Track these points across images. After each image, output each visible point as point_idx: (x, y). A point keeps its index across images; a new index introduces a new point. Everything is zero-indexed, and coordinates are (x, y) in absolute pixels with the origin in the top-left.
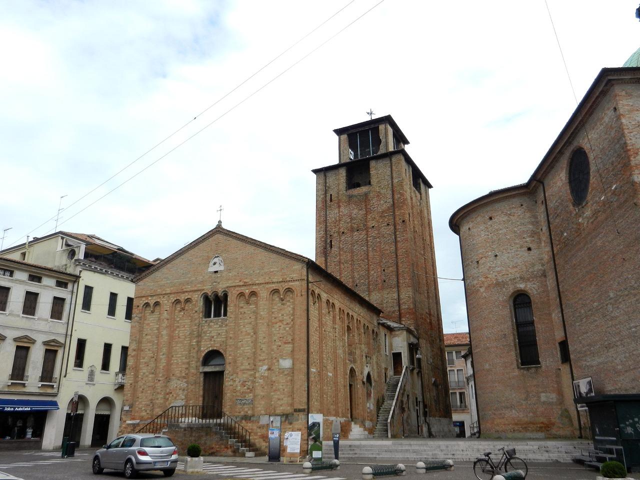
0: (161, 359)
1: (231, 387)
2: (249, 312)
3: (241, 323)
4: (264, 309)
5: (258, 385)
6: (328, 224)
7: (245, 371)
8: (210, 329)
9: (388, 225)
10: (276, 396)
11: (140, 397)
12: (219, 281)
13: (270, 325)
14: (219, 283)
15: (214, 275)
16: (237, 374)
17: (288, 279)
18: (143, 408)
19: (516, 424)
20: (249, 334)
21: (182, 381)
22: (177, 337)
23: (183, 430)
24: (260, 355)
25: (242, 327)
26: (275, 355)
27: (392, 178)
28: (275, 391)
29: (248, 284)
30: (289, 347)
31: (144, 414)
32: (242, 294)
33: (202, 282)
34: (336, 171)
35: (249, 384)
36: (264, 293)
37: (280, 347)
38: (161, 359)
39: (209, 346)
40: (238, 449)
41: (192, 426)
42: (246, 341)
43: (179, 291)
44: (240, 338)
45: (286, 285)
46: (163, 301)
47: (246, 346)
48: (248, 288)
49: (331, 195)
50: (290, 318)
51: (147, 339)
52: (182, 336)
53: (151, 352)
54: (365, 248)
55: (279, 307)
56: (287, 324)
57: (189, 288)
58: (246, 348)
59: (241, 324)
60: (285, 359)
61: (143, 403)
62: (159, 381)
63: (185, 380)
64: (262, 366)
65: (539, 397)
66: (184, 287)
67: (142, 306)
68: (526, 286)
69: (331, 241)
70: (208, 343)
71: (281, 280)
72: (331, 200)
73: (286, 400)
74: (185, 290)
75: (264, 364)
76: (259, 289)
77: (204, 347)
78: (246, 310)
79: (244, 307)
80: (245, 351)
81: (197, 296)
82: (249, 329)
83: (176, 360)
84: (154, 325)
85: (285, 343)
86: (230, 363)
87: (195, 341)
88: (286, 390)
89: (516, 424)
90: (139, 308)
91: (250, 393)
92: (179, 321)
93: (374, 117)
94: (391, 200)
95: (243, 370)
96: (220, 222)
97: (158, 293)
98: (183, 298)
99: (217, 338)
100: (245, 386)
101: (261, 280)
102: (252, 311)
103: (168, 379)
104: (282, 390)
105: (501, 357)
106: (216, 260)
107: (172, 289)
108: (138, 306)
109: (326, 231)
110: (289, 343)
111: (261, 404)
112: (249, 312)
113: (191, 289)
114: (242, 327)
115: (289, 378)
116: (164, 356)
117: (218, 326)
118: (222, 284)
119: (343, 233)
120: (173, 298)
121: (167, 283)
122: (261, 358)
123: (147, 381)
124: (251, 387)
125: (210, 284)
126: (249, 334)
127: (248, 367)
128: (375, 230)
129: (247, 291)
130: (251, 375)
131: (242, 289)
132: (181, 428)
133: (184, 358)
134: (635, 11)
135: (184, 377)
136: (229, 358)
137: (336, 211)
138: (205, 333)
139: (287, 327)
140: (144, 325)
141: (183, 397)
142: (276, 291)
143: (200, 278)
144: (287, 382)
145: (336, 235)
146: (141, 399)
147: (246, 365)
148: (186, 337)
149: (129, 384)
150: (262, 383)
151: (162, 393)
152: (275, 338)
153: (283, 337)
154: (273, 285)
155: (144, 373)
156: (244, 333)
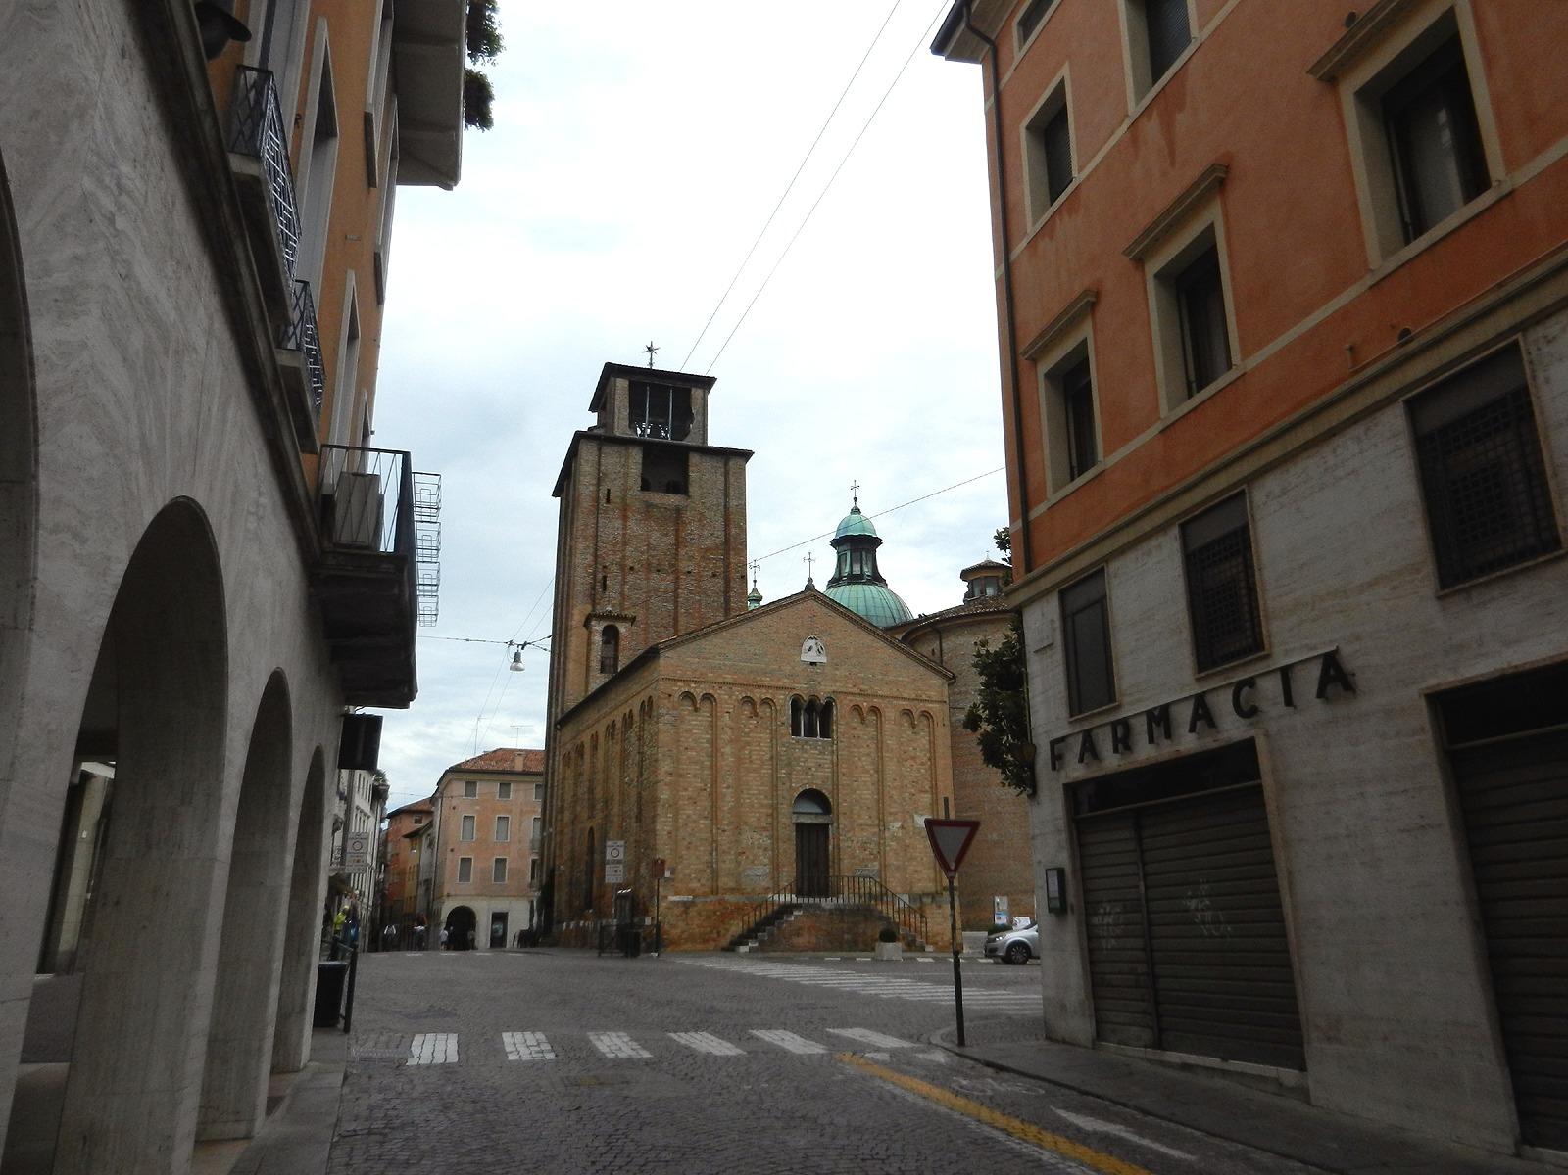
0: (725, 796)
5: (891, 850)
6: (600, 544)
8: (805, 755)
9: (714, 575)
11: (685, 857)
12: (820, 679)
13: (900, 762)
17: (924, 697)
18: (693, 876)
20: (868, 771)
21: (762, 835)
23: (827, 913)
25: (856, 759)
27: (727, 496)
31: (695, 885)
32: (857, 708)
34: (622, 449)
35: (872, 846)
36: (890, 713)
39: (806, 782)
40: (915, 940)
41: (842, 907)
43: (750, 682)
45: (922, 707)
49: (609, 490)
50: (925, 755)
51: (689, 758)
54: (671, 607)
56: (922, 764)
57: (767, 681)
62: (724, 831)
66: (759, 678)
67: (677, 695)
69: (605, 578)
70: (803, 777)
71: (914, 696)
72: (608, 501)
74: (760, 683)
77: (796, 783)
79: (859, 728)
82: (866, 763)
83: (749, 799)
85: (922, 791)
86: (845, 813)
87: (784, 771)
88: (925, 859)
94: (721, 533)
96: (810, 580)
97: (709, 679)
98: (758, 696)
99: (817, 770)
101: (885, 691)
103: (738, 830)
104: (919, 859)
105: (1021, 827)
106: (812, 643)
108: (670, 696)
109: (596, 556)
113: (773, 684)
116: (730, 790)
119: (632, 568)
120: (739, 693)
121: (725, 665)
122: (892, 810)
124: (875, 852)
126: (868, 771)
127: (869, 822)
130: (874, 834)
131: (859, 700)
132: (824, 910)
133: (762, 797)
134: (494, 91)
135: (764, 828)
136: (843, 803)
137: (618, 523)
138: (797, 759)
141: (766, 861)
142: (908, 713)
143: (787, 669)
145: (614, 568)
147: (865, 819)
151: (732, 852)
152: (906, 782)
155: (689, 816)
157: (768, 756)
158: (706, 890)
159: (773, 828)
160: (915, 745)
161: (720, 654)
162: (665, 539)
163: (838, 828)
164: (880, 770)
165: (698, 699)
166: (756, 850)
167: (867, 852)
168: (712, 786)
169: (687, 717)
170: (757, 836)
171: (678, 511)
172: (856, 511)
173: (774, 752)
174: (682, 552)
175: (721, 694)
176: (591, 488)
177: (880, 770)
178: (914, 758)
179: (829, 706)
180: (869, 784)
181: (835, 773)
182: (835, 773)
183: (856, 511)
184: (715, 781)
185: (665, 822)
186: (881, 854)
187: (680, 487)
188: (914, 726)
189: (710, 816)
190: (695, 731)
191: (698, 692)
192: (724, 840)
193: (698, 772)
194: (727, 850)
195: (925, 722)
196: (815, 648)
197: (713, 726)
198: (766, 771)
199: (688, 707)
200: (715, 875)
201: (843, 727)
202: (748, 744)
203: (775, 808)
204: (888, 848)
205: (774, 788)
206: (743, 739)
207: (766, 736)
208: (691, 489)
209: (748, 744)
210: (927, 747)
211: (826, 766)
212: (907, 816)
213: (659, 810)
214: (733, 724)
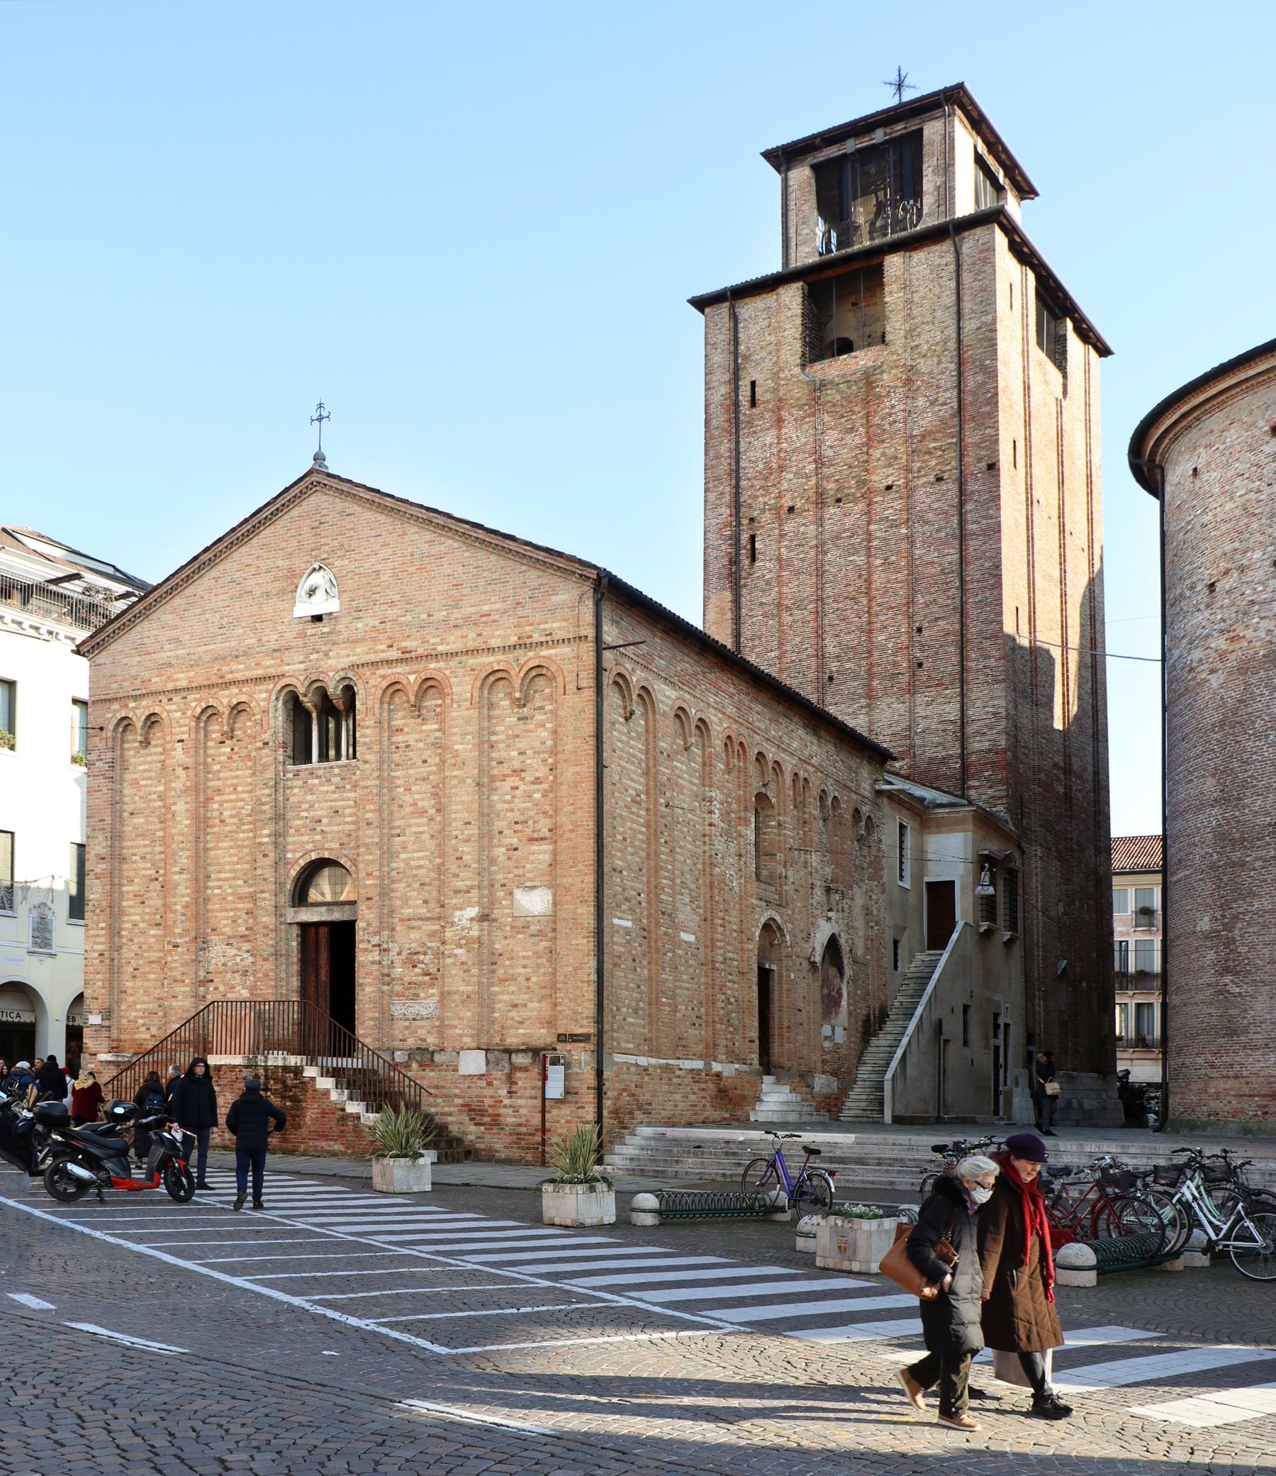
7: (415, 923)
8: (309, 798)
10: (506, 997)
14: (326, 654)
15: (312, 629)
16: (393, 929)
21: (239, 949)
22: (217, 821)
24: (456, 876)
29: (413, 655)
35: (427, 959)
37: (516, 853)
39: (310, 846)
43: (214, 680)
52: (231, 816)
53: (149, 865)
55: (510, 727)
56: (537, 781)
58: (416, 855)
63: (246, 946)
64: (461, 909)
66: (225, 669)
74: (229, 677)
75: (470, 905)
76: (447, 672)
78: (411, 738)
79: (406, 729)
81: (264, 695)
83: (219, 887)
88: (534, 979)
91: (432, 985)
92: (219, 771)
95: (409, 920)
98: (225, 701)
100: (414, 966)
101: (454, 642)
104: (521, 980)
110: (542, 839)
111: (461, 1019)
112: (421, 745)
118: (338, 656)
123: (145, 947)
125: (301, 658)
127: (423, 911)
129: (412, 678)
130: (432, 935)
135: (242, 937)
139: (538, 791)
144: (539, 957)
150: (464, 959)
151: (187, 981)
154: (492, 659)
156: (408, 810)
167: (417, 970)
193: (148, 849)
194: (179, 978)
201: (368, 731)
211: (347, 811)
212: (500, 894)
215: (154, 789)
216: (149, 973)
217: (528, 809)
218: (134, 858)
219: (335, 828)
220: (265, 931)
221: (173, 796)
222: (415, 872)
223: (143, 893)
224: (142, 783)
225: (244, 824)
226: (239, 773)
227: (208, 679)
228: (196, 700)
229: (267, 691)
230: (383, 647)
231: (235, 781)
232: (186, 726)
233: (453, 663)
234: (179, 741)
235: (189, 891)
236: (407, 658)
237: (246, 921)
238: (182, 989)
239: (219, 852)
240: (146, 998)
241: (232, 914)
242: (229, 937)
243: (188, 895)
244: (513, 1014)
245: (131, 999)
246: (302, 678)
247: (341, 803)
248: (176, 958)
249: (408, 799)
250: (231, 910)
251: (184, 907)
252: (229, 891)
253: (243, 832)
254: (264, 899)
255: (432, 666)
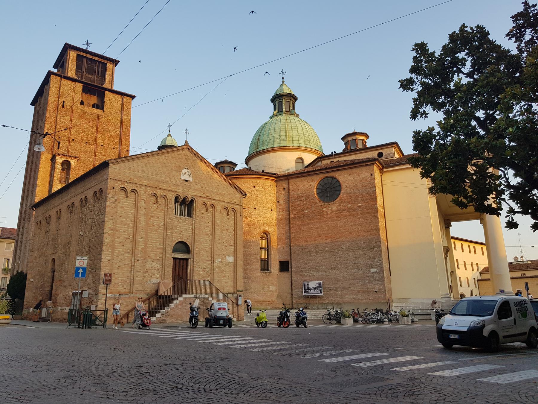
0: (139, 242)
1: (198, 271)
2: (207, 218)
3: (202, 225)
4: (219, 219)
7: (205, 261)
8: (179, 225)
10: (224, 281)
15: (185, 183)
17: (233, 202)
18: (120, 284)
19: (256, 302)
21: (156, 263)
22: (152, 225)
24: (216, 251)
25: (203, 228)
26: (223, 252)
28: (224, 277)
30: (232, 248)
32: (205, 204)
33: (175, 185)
36: (218, 208)
38: (139, 242)
39: (179, 237)
42: (206, 239)
44: (202, 236)
46: (140, 190)
47: (206, 242)
48: (209, 201)
49: (64, 102)
53: (126, 234)
55: (225, 219)
56: (231, 232)
57: (164, 186)
59: (202, 226)
60: (230, 256)
61: (119, 279)
63: (159, 262)
64: (217, 259)
65: (269, 288)
66: (159, 184)
68: (268, 230)
71: (229, 201)
72: (63, 107)
73: (231, 284)
74: (160, 187)
80: (205, 246)
82: (207, 230)
83: (151, 244)
84: (129, 210)
87: (169, 231)
89: (256, 302)
90: (114, 190)
91: (208, 277)
92: (153, 211)
93: (90, 49)
98: (159, 193)
102: (210, 218)
104: (227, 277)
106: (186, 171)
107: (149, 182)
108: (114, 188)
112: (207, 218)
114: (203, 228)
115: (231, 269)
117: (186, 224)
119: (73, 140)
120: (150, 191)
121: (144, 176)
125: (182, 189)
128: (103, 149)
130: (209, 264)
131: (205, 200)
133: (158, 244)
135: (158, 260)
137: (68, 118)
138: (176, 226)
140: (118, 207)
141: (158, 276)
146: (117, 275)
148: (159, 227)
149: (107, 260)
150: (218, 271)
151: (142, 272)
153: (228, 241)
155: (120, 252)
156: (204, 233)
157: (162, 224)
158: (127, 291)
159: (163, 258)
160: (228, 224)
161: (141, 170)
162: (91, 128)
163: (193, 261)
164: (213, 234)
165: (129, 191)
166: (153, 271)
168: (133, 237)
169: (122, 200)
170: (155, 264)
171: (98, 118)
172: (169, 135)
173: (166, 222)
174: (99, 136)
175: (141, 190)
176: (55, 99)
177: (213, 234)
178: (227, 230)
179: (192, 201)
180: (208, 240)
181: (194, 234)
182: (194, 234)
183: (169, 135)
184: (135, 234)
185: (107, 254)
186: (212, 274)
187: (100, 106)
188: (228, 215)
189: (131, 253)
190: (125, 208)
191: (129, 188)
192: (137, 265)
193: (126, 229)
194: (139, 270)
195: (233, 214)
196: (187, 174)
197: (136, 206)
198: (161, 231)
199: (123, 194)
200: (132, 283)
202: (153, 217)
203: (164, 250)
204: (214, 271)
205: (165, 239)
206: (150, 214)
207: (162, 214)
208: (105, 108)
209: (153, 217)
210: (233, 225)
213: (104, 248)
214: (146, 206)
215: (130, 211)
216: (124, 268)
217: (229, 238)
218: (121, 231)
219: (186, 234)
220: (168, 259)
221: (140, 215)
222: (205, 248)
223: (123, 242)
224: (125, 208)
225: (160, 228)
226: (160, 213)
227: (154, 185)
228: (149, 190)
229: (172, 194)
230: (202, 193)
231: (158, 215)
232: (146, 196)
233: (217, 202)
234: (143, 200)
235: (144, 244)
236: (207, 198)
237: (159, 255)
238: (140, 274)
239: (152, 234)
240: (123, 276)
241: (155, 253)
242: (153, 259)
243: (143, 246)
244: (226, 285)
245: (117, 276)
246: (182, 194)
247: (188, 228)
248: (138, 264)
249: (204, 230)
250: (155, 251)
251: (141, 249)
252: (155, 246)
253: (160, 230)
254: (168, 250)
255: (213, 201)
